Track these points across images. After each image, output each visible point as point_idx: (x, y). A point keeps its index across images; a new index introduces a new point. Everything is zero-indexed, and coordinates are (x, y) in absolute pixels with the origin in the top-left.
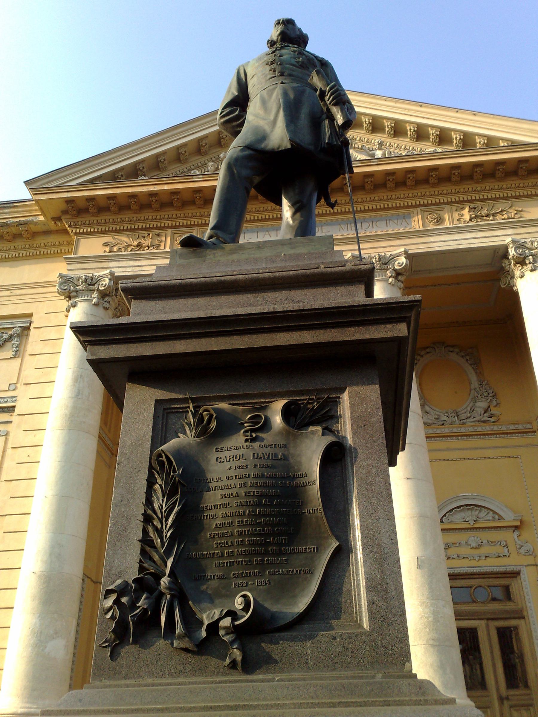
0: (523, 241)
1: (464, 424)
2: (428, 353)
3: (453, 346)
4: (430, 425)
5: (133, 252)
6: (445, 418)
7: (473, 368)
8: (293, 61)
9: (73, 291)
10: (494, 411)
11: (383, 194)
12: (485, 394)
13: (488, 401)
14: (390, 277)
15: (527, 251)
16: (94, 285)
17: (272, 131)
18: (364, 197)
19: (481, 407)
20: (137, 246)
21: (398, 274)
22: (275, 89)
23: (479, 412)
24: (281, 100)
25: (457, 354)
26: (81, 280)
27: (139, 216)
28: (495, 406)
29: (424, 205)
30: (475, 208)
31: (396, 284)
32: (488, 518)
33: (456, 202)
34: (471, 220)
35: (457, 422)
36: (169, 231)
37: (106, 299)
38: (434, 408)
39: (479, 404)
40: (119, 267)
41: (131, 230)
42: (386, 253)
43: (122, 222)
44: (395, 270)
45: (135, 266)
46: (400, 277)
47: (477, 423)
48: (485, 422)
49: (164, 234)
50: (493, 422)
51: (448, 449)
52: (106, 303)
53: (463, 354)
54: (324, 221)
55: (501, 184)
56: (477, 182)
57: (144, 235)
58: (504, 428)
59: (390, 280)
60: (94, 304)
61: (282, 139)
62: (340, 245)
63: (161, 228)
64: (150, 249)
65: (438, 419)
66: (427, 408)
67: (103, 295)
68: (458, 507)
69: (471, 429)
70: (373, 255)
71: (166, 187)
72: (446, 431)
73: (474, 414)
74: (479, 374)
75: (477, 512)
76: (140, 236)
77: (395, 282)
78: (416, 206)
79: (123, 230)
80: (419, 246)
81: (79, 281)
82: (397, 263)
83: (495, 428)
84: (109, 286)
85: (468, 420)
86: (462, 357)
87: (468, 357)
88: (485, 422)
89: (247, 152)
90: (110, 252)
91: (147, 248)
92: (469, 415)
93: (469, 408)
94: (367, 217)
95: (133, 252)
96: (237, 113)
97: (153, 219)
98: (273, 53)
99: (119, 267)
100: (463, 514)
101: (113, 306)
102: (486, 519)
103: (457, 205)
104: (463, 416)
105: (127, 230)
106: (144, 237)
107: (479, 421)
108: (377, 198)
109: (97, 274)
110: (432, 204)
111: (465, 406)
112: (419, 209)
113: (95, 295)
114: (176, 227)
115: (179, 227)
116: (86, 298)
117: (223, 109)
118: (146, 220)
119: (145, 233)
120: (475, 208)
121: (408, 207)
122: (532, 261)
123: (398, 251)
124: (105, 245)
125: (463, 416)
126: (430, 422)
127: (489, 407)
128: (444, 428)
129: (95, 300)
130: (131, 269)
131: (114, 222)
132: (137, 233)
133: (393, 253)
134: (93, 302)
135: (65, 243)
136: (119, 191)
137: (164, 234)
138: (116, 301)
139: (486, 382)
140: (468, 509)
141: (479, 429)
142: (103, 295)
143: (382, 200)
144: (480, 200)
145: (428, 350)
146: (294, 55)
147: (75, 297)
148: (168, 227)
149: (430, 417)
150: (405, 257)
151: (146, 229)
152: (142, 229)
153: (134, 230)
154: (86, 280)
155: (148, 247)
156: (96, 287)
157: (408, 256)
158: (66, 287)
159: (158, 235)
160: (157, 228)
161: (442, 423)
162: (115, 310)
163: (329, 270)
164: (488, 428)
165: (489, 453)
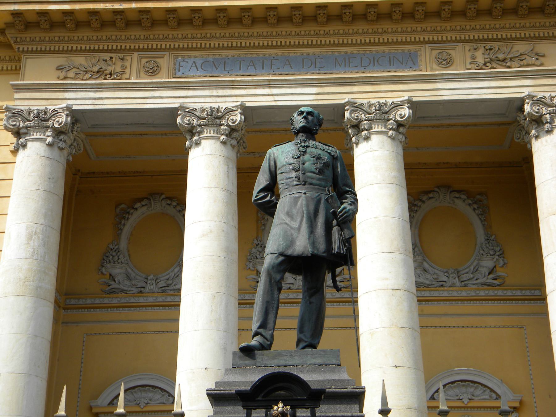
0: (540, 95)
1: (466, 286)
2: (430, 198)
3: (459, 191)
4: (428, 286)
5: (93, 82)
6: (445, 279)
7: (480, 219)
8: (313, 170)
9: (23, 127)
10: (501, 272)
11: (386, 25)
12: (492, 253)
13: (495, 260)
14: (390, 129)
15: (544, 109)
16: (47, 120)
17: (297, 237)
18: (366, 27)
19: (486, 267)
20: (98, 72)
21: (399, 125)
22: (300, 197)
23: (483, 272)
24: (305, 212)
25: (464, 201)
26: (32, 115)
27: (99, 34)
28: (502, 267)
29: (434, 42)
30: (491, 49)
31: (397, 137)
32: (484, 397)
33: (470, 41)
34: (485, 64)
35: (458, 284)
36: (136, 55)
37: (62, 137)
38: (434, 266)
39: (484, 263)
40: (76, 99)
41: (90, 51)
42: (388, 100)
43: (80, 40)
44: (396, 121)
45: (95, 99)
46: (401, 129)
47: (481, 287)
48: (488, 285)
49: (129, 58)
50: (498, 285)
51: (446, 315)
52: (61, 143)
53: (470, 202)
54: (317, 54)
55: (523, 22)
56: (496, 18)
57: (105, 58)
58: (509, 293)
59: (391, 132)
60: (47, 145)
61: (305, 247)
62: (336, 86)
63: (125, 50)
64: (112, 77)
65: (436, 279)
66: (426, 265)
67: (58, 133)
68: (453, 383)
69: (472, 293)
70: (373, 101)
71: (134, 5)
72: (445, 294)
73: (478, 275)
74: (487, 227)
75: (472, 390)
76: (101, 60)
77: (396, 135)
78: (425, 42)
79: (81, 51)
80: (425, 93)
81: (29, 115)
82: (399, 113)
83: (500, 293)
84: (66, 124)
85: (470, 282)
86: (470, 205)
87: (475, 206)
88: (488, 285)
89: (281, 258)
90: (65, 78)
91: (109, 76)
92: (472, 276)
93: (472, 268)
94: (368, 52)
95: (93, 82)
96: (268, 198)
97: (118, 39)
98: (298, 158)
99: (76, 99)
100: (457, 391)
101: (69, 142)
102: (482, 397)
103: (471, 44)
104: (465, 277)
105: (85, 51)
106: (105, 61)
107: (483, 284)
108: (380, 30)
109: (52, 108)
110: (442, 42)
111: (468, 264)
112: (427, 46)
113: (49, 133)
114: (143, 50)
115: (148, 50)
116: (38, 136)
117: (258, 193)
118: (108, 39)
119: (107, 57)
120: (491, 49)
121: (415, 43)
122: (549, 121)
123: (401, 99)
124: (60, 68)
125: (465, 277)
126: (427, 282)
127: (495, 267)
128: (443, 290)
129: (50, 139)
130: (90, 102)
131: (70, 40)
132: (97, 55)
133: (396, 100)
134: (47, 142)
135: (7, 58)
136: (77, 7)
137: (129, 58)
138: (72, 137)
139: (493, 237)
140: (463, 385)
141: (482, 293)
142: (58, 133)
143: (385, 32)
144: (497, 40)
145: (431, 195)
146: (314, 160)
147: (26, 134)
148: (134, 50)
149: (428, 276)
150: (408, 107)
151: (108, 51)
152: (103, 51)
153: (94, 51)
154: (38, 116)
155: (111, 74)
156: (50, 124)
157: (412, 105)
158: (14, 123)
159: (122, 59)
160: (121, 51)
161: (441, 283)
162: (70, 146)
163: (337, 390)
164: (491, 293)
165: (491, 321)
